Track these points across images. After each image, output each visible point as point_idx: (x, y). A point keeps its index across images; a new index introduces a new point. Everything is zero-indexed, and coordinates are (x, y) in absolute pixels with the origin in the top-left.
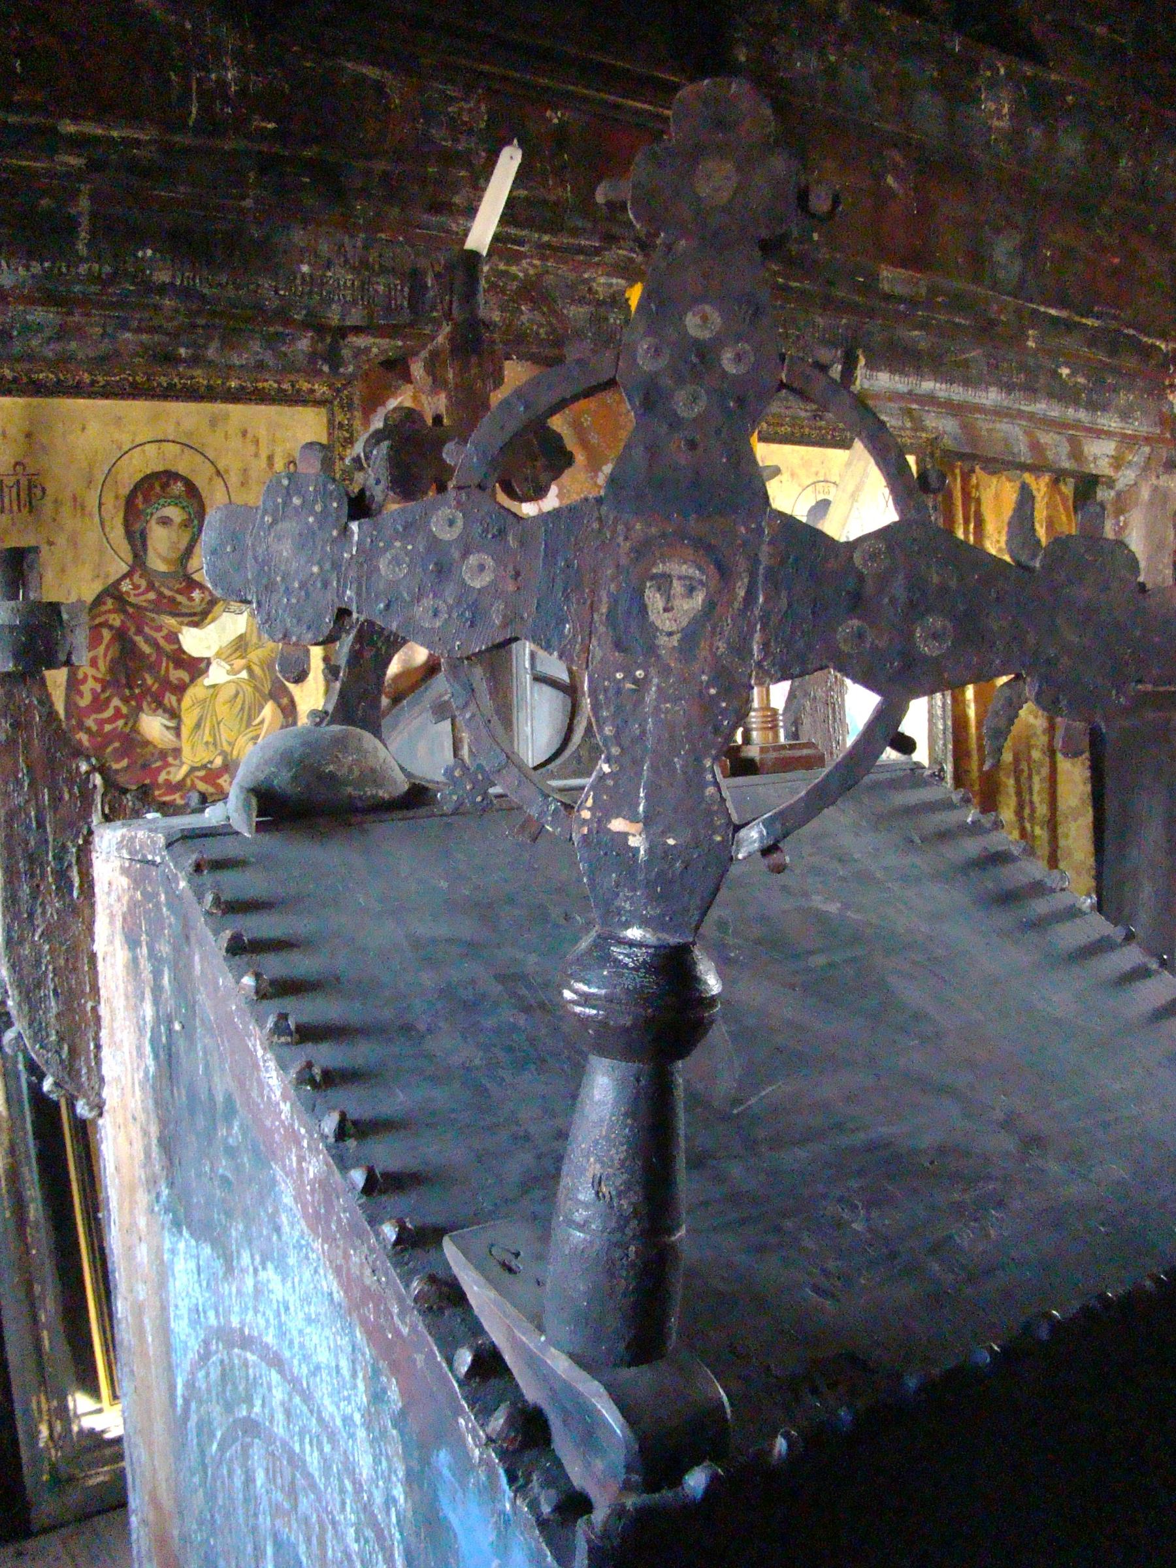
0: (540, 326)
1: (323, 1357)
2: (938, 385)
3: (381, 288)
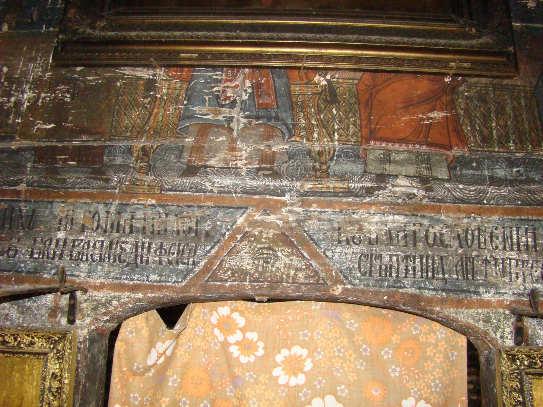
0: (297, 270)
3: (128, 247)
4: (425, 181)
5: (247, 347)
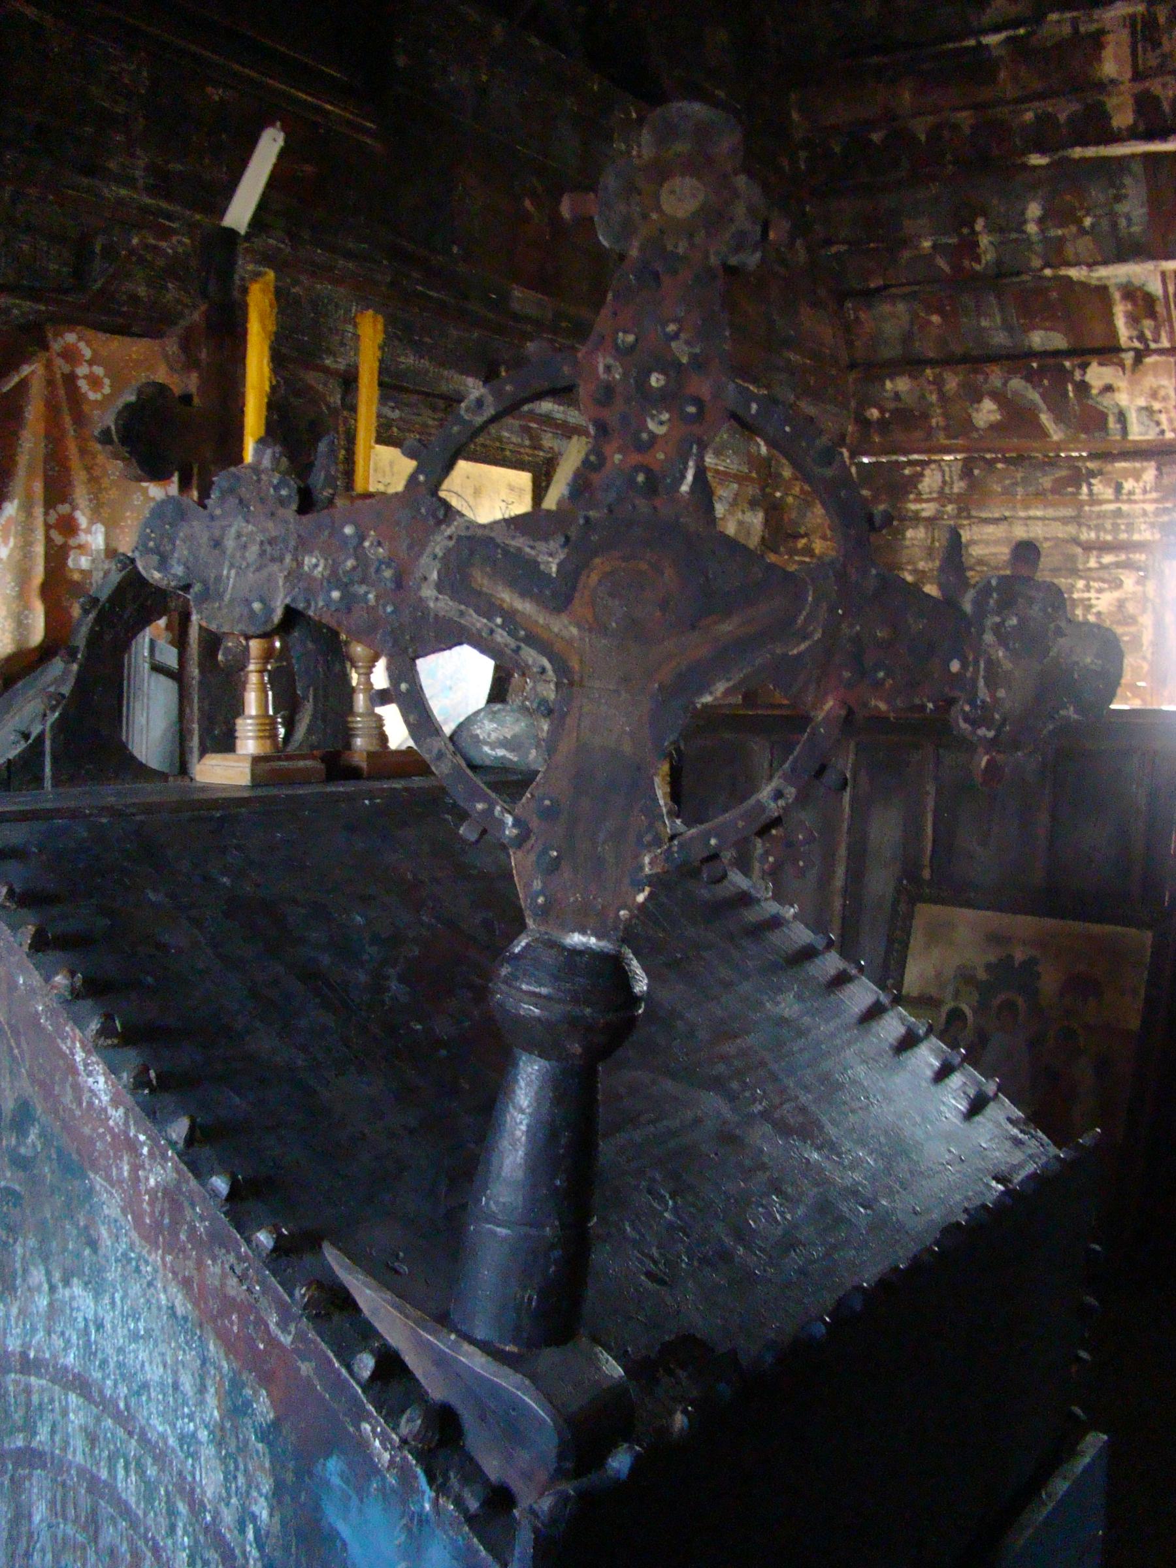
1: (154, 1373)
2: (556, 406)
4: (293, 237)
5: (95, 382)
